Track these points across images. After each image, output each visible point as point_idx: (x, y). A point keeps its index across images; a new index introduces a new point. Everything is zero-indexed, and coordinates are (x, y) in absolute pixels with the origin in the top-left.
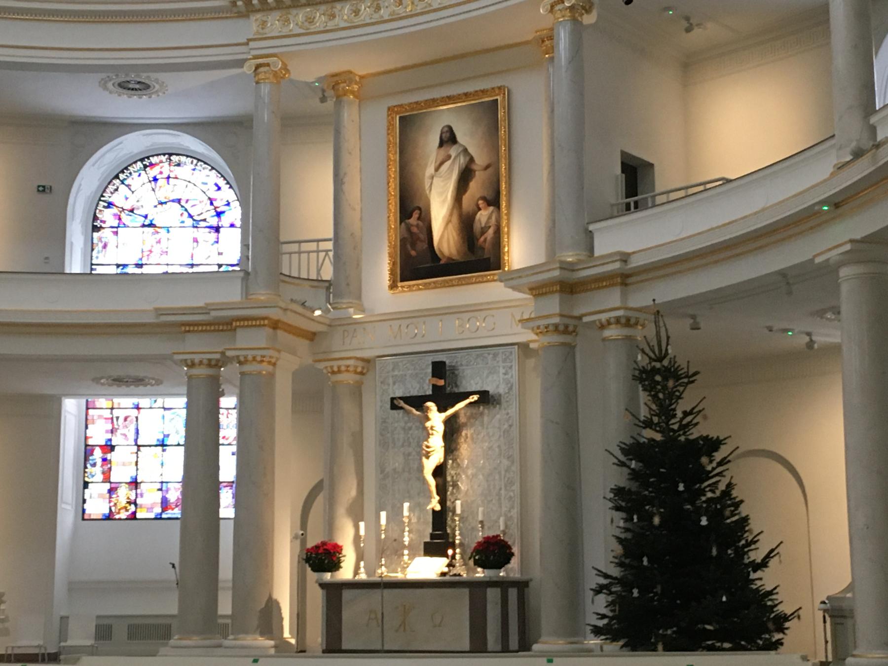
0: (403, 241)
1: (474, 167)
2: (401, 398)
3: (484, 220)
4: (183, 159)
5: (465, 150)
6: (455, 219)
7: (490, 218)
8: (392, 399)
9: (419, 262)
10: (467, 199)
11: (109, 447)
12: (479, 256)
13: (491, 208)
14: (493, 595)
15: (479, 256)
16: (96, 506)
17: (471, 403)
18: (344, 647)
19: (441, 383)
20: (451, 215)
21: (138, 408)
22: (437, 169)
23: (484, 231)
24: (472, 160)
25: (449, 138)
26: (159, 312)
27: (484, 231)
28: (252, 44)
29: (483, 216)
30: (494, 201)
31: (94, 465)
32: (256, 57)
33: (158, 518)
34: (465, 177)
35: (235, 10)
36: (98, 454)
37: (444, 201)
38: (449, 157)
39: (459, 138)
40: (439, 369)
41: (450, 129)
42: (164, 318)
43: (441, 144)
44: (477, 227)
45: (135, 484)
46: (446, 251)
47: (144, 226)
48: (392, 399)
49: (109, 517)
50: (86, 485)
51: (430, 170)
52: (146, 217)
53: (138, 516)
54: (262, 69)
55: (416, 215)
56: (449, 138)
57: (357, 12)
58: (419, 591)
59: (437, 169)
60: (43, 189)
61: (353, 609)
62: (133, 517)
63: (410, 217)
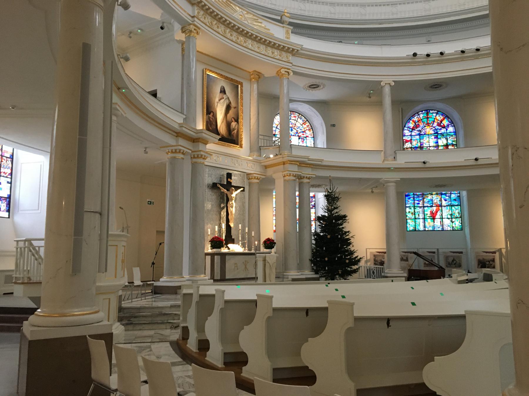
0: (207, 122)
3: (234, 126)
5: (228, 98)
6: (225, 121)
12: (231, 138)
14: (217, 258)
15: (231, 138)
18: (227, 277)
22: (220, 100)
23: (234, 130)
24: (230, 103)
25: (223, 91)
27: (234, 130)
29: (234, 124)
30: (237, 121)
34: (228, 108)
37: (221, 113)
38: (223, 98)
39: (227, 92)
43: (221, 92)
51: (217, 100)
55: (212, 114)
56: (223, 91)
58: (250, 256)
59: (220, 100)
63: (210, 114)
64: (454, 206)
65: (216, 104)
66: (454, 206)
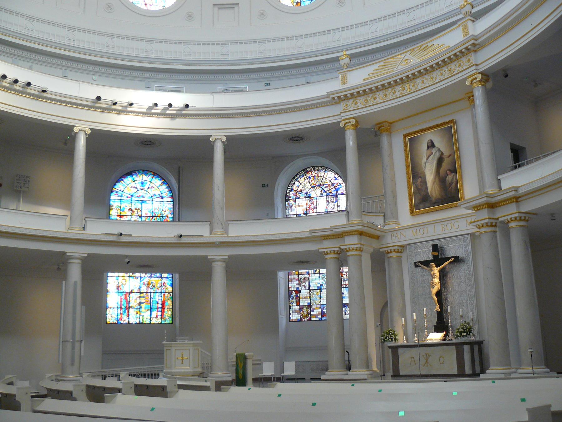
1: (444, 156)
2: (419, 262)
4: (320, 168)
5: (439, 150)
6: (437, 180)
7: (453, 178)
8: (415, 263)
9: (422, 201)
10: (442, 171)
11: (298, 291)
12: (450, 195)
13: (453, 174)
14: (466, 348)
15: (450, 195)
16: (295, 316)
17: (451, 262)
18: (401, 374)
19: (436, 254)
20: (435, 179)
21: (309, 274)
22: (427, 159)
23: (451, 184)
24: (442, 153)
25: (431, 145)
26: (311, 231)
27: (451, 184)
28: (342, 115)
29: (449, 178)
30: (454, 171)
31: (293, 299)
32: (345, 120)
33: (320, 320)
35: (334, 101)
36: (294, 293)
37: (431, 173)
38: (432, 153)
39: (436, 144)
40: (435, 248)
41: (432, 141)
42: (313, 234)
43: (428, 148)
44: (447, 182)
45: (310, 306)
46: (434, 195)
47: (306, 197)
48: (415, 263)
49: (300, 320)
50: (290, 307)
51: (424, 160)
52: (307, 193)
53: (312, 319)
54: (347, 125)
55: (420, 180)
56: (431, 145)
57: (386, 95)
60: (264, 186)
61: (404, 357)
62: (310, 320)
64: (163, 312)
65: (423, 166)
66: (163, 312)
